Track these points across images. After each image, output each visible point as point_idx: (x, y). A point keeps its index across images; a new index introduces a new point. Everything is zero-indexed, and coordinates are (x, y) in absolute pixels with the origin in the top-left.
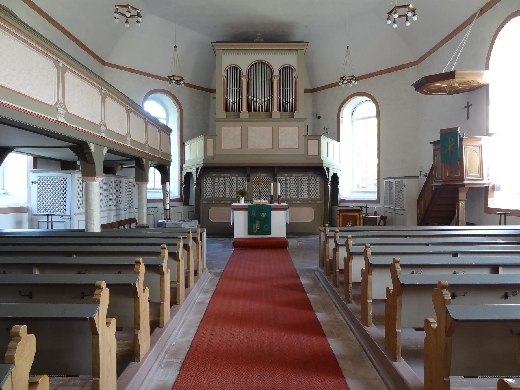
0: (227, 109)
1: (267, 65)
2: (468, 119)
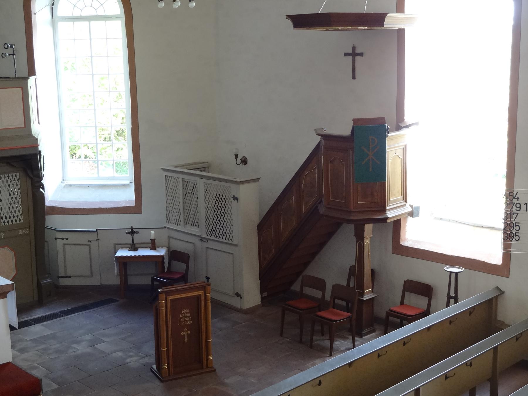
2: (354, 78)
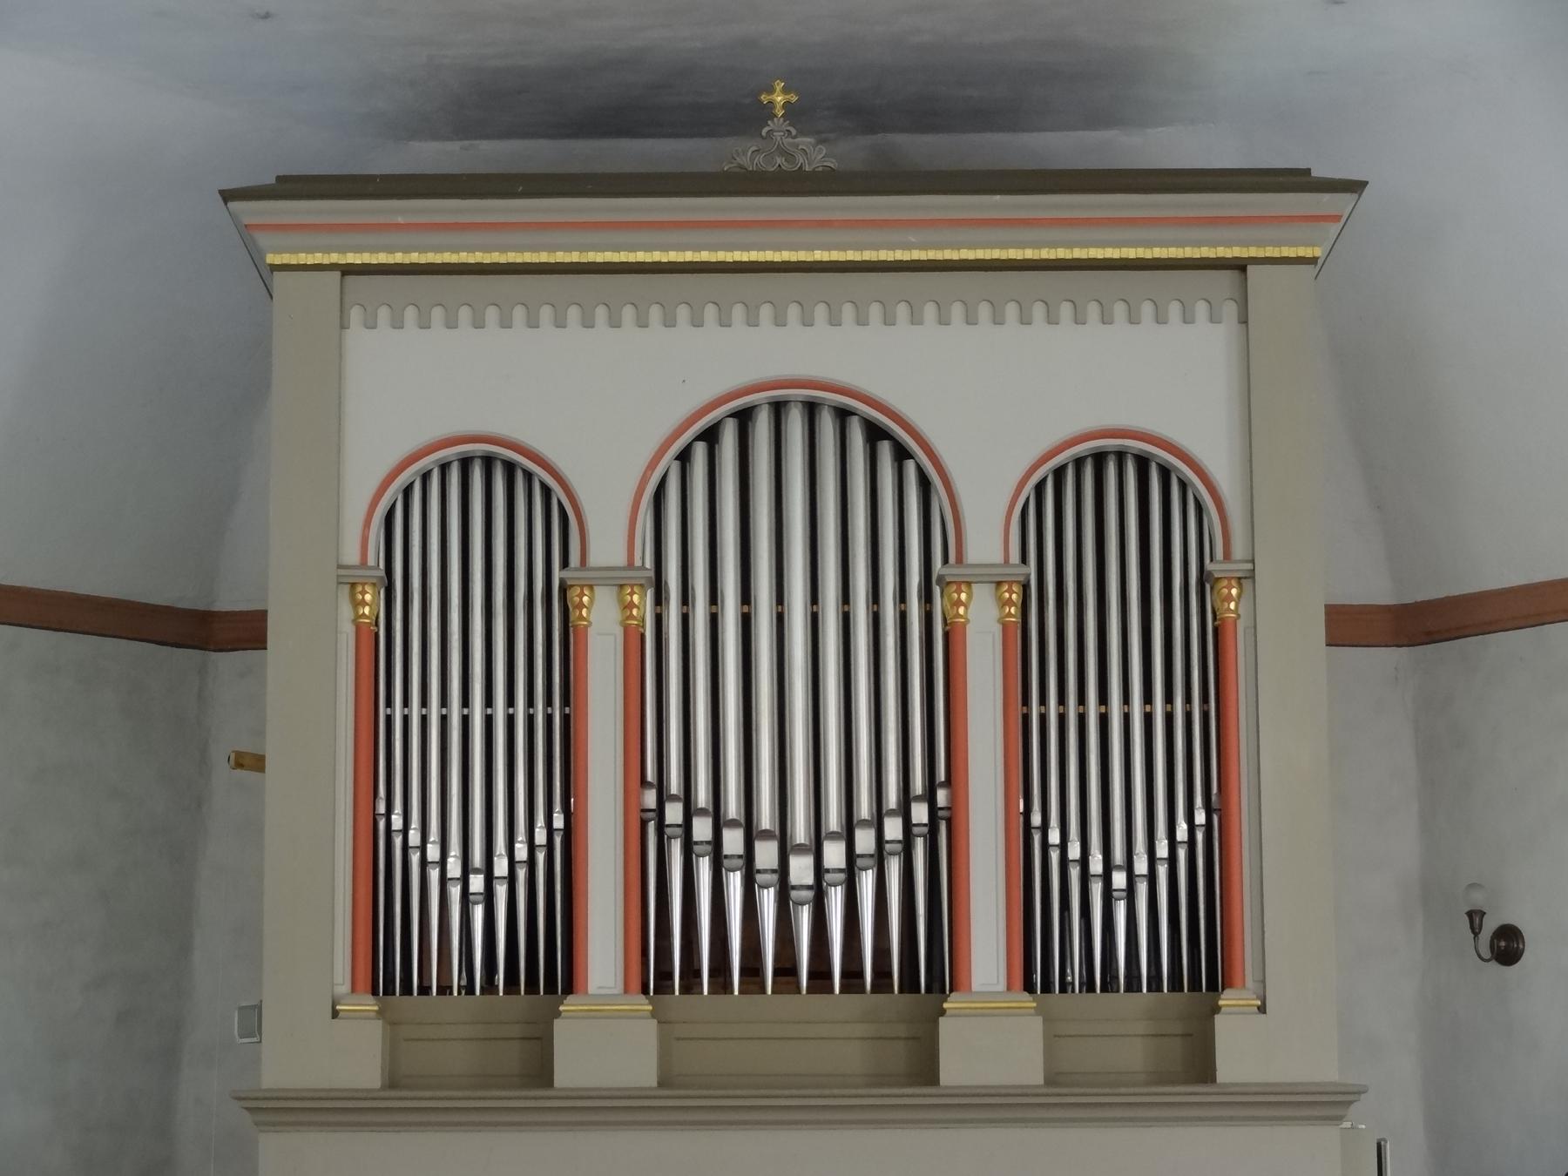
0: (390, 963)
1: (875, 433)
